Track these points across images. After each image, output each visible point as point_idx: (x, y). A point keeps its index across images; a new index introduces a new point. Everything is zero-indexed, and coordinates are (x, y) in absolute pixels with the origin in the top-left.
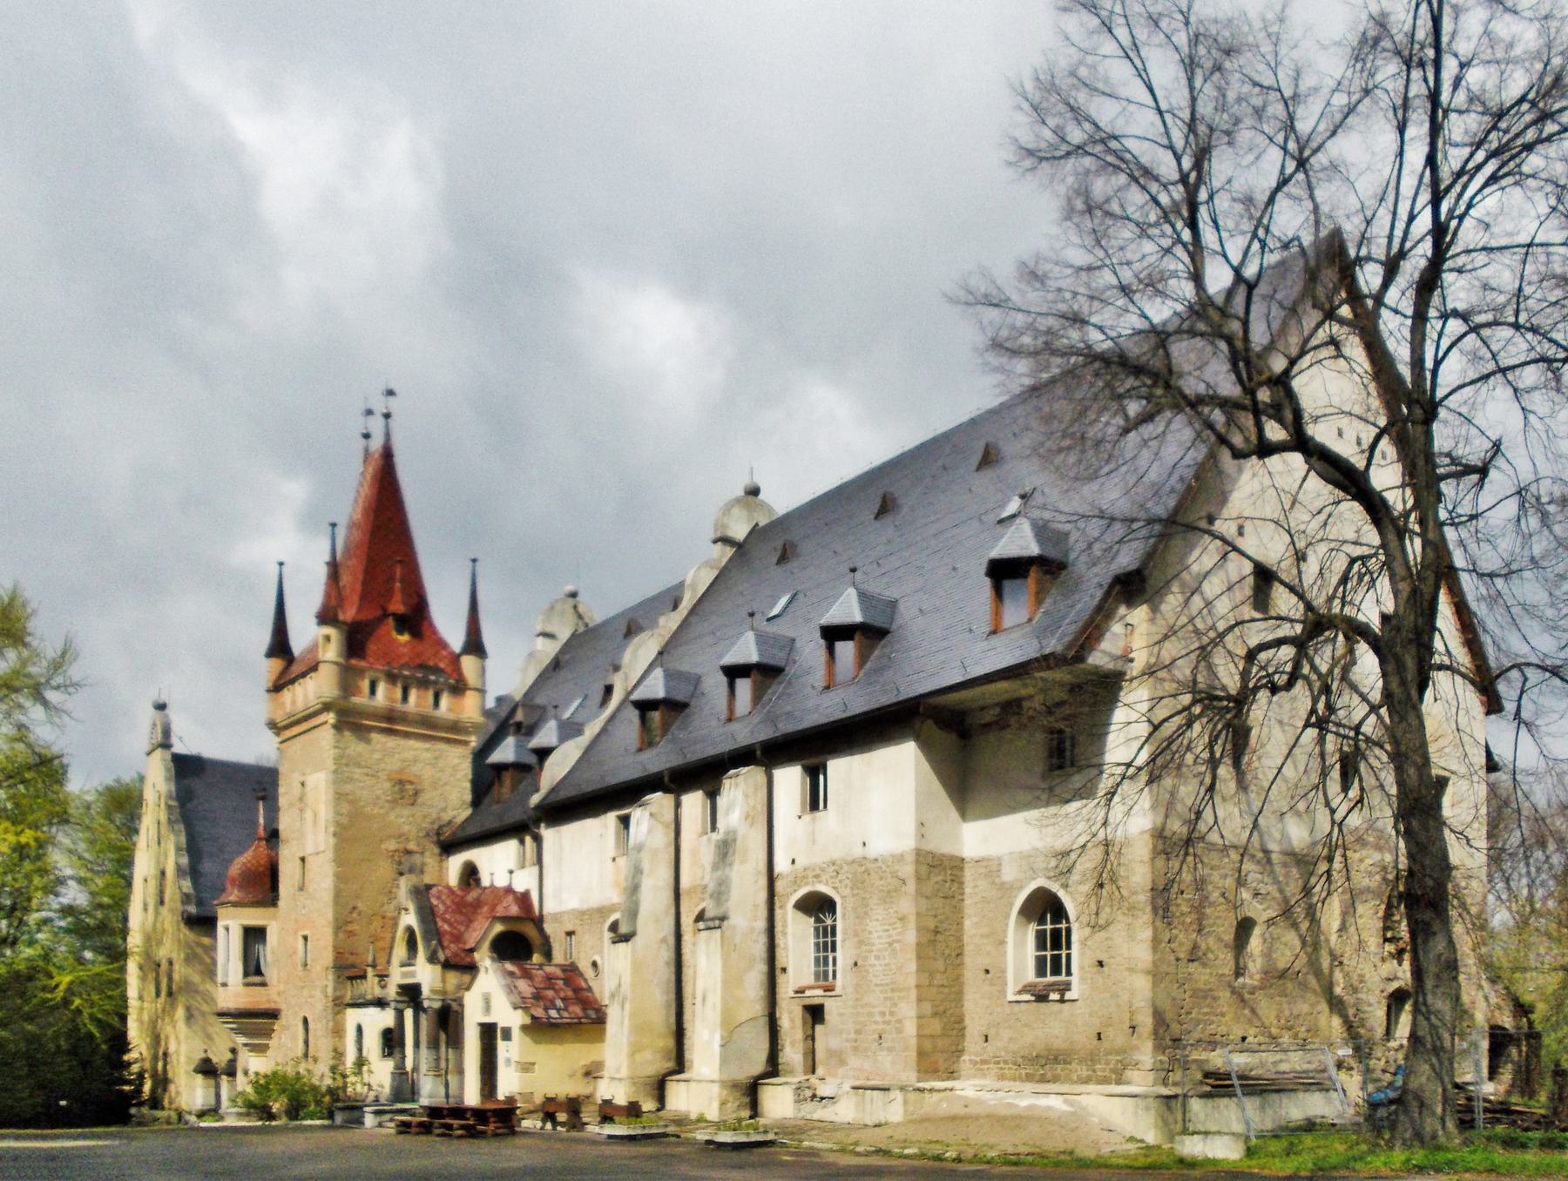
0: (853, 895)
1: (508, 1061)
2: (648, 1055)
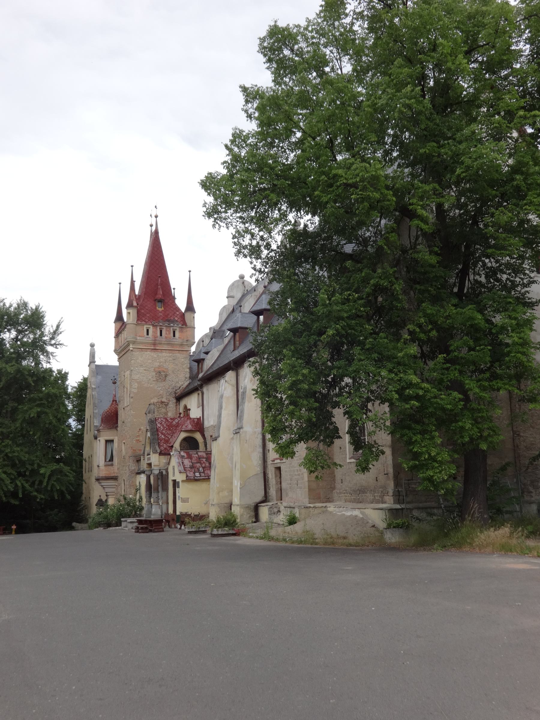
1: (179, 497)
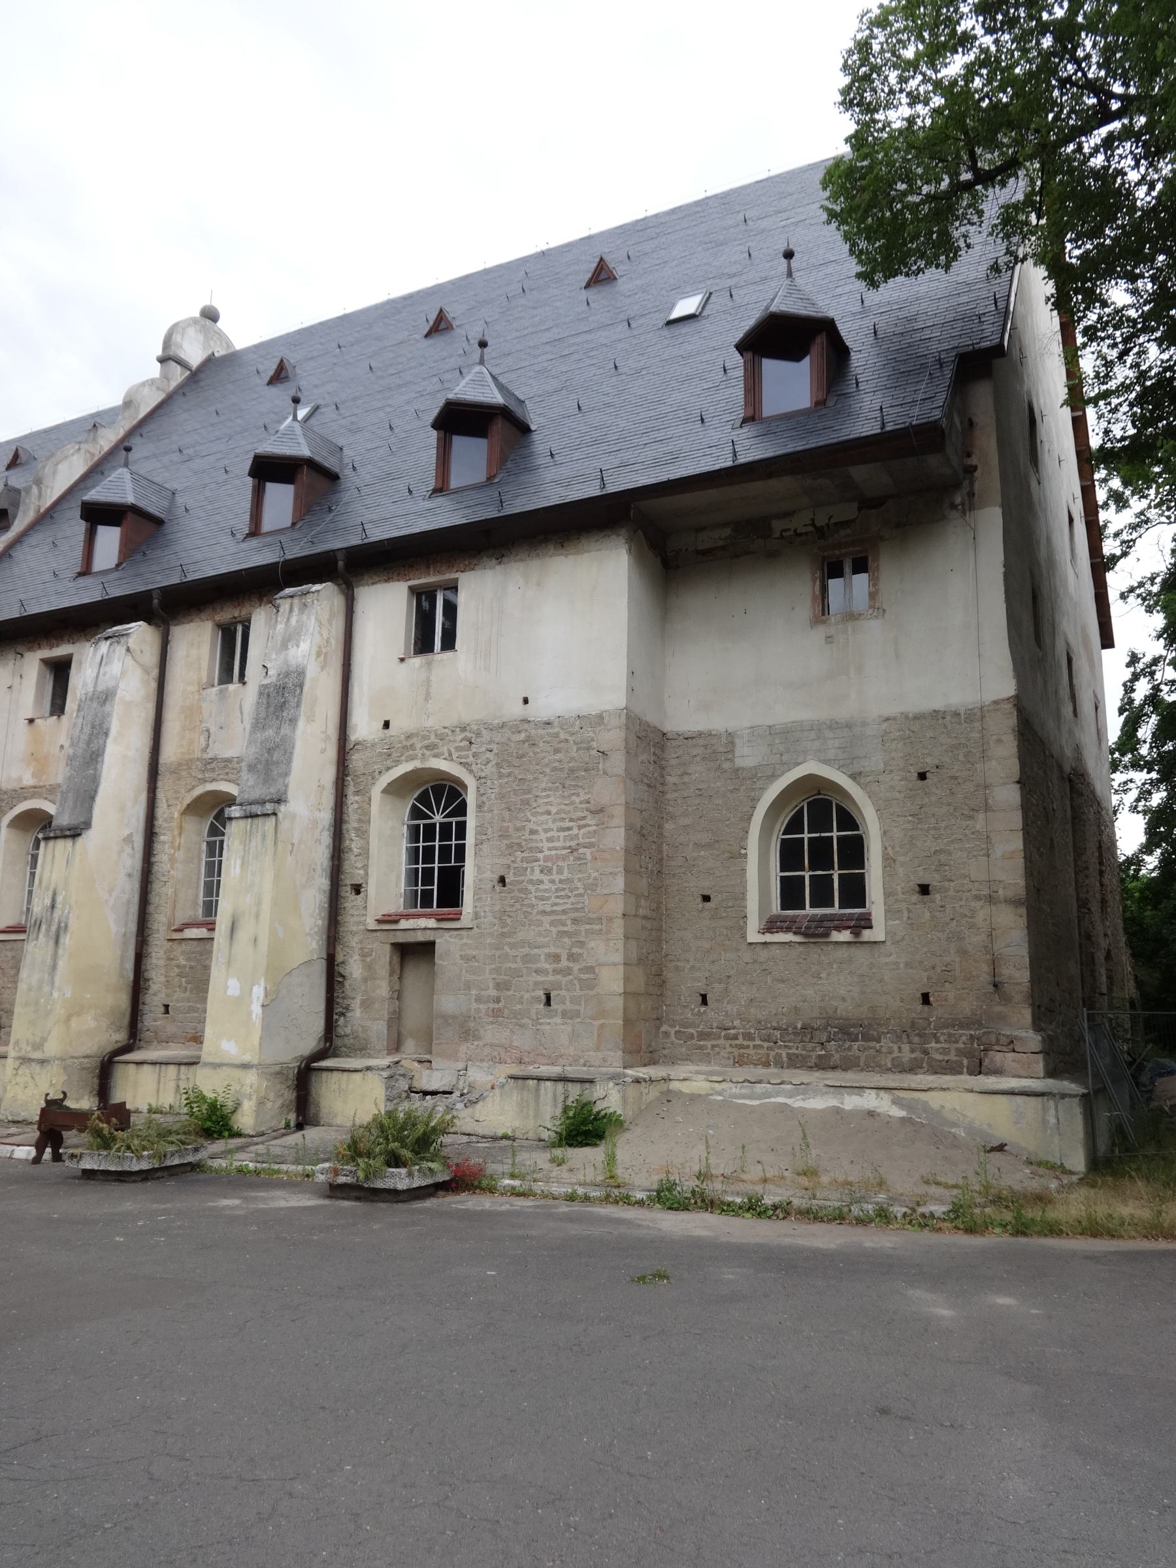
0: (501, 776)
2: (88, 1021)
